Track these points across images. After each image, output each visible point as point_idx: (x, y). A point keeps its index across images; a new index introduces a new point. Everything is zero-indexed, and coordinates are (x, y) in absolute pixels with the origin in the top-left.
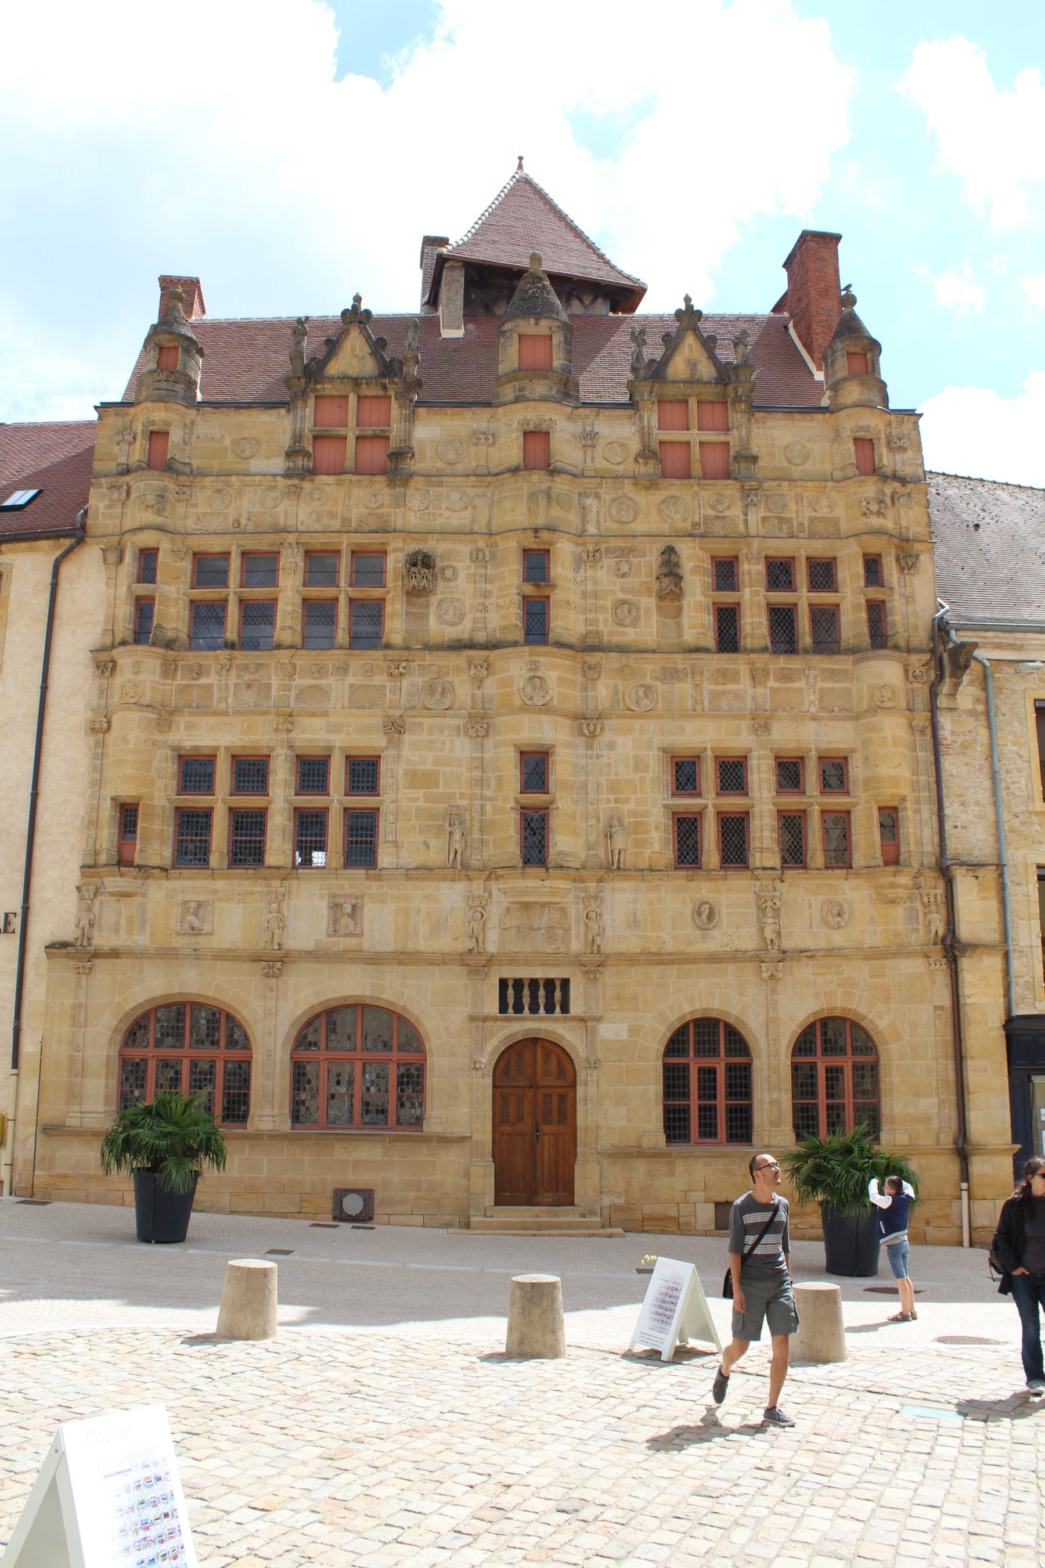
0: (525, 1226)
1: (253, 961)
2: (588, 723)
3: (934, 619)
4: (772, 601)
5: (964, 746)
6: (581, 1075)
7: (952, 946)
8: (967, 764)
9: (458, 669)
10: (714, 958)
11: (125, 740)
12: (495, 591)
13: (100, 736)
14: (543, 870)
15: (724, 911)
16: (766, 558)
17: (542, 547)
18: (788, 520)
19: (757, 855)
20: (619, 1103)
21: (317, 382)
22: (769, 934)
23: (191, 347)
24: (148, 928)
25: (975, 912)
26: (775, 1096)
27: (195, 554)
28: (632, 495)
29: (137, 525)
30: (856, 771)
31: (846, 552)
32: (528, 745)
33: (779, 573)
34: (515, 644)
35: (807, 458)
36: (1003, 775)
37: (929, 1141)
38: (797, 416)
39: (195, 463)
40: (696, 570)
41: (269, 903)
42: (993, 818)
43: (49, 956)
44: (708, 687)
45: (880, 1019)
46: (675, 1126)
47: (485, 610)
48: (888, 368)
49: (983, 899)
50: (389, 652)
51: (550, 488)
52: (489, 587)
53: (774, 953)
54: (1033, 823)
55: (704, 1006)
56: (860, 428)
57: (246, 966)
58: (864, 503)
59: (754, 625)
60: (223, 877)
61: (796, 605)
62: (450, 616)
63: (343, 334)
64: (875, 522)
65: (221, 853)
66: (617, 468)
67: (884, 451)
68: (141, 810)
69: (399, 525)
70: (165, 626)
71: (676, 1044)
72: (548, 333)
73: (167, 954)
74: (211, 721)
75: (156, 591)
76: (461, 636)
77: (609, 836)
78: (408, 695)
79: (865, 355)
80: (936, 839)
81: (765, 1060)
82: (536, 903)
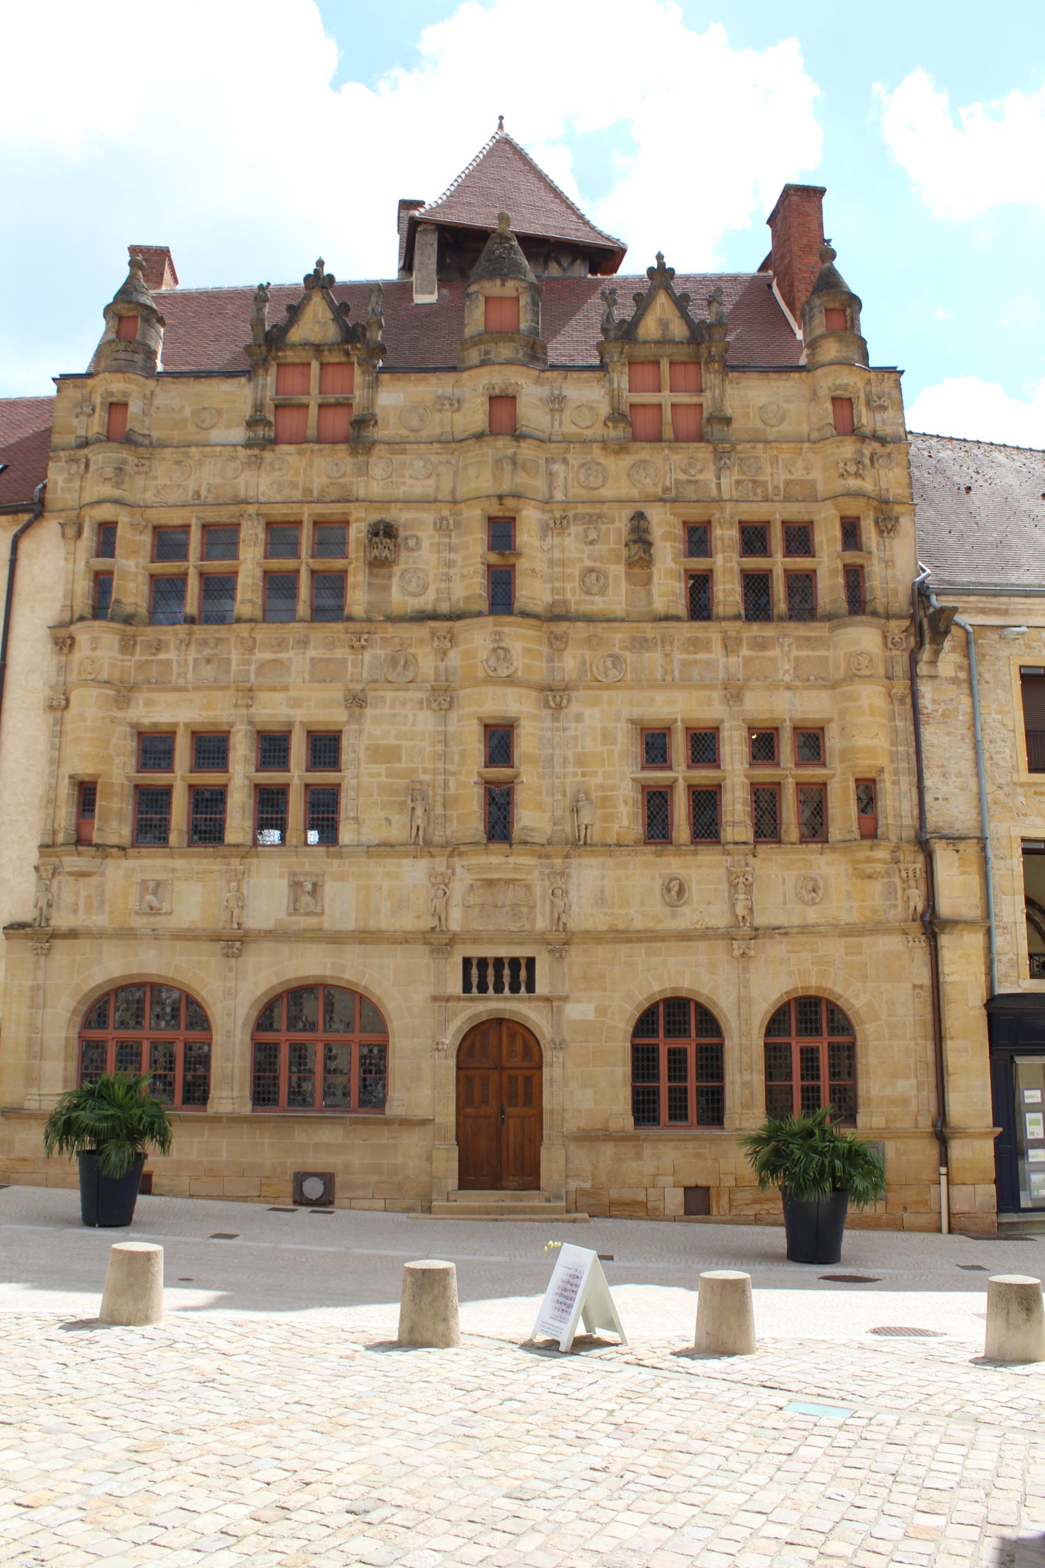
0: (487, 1211)
1: (212, 940)
2: (554, 694)
3: (914, 584)
4: (746, 567)
5: (945, 715)
6: (547, 1056)
7: (931, 923)
8: (948, 734)
9: (421, 641)
10: (684, 936)
11: (83, 718)
12: (459, 563)
13: (59, 714)
14: (507, 846)
15: (694, 887)
16: (740, 522)
17: (507, 514)
18: (764, 484)
19: (729, 829)
20: (586, 1084)
21: (278, 350)
22: (740, 911)
23: (151, 316)
24: (107, 908)
25: (955, 887)
26: (747, 1077)
27: (155, 528)
28: (601, 460)
29: (95, 499)
30: (833, 742)
31: (823, 515)
32: (491, 718)
33: (754, 538)
34: (479, 614)
35: (783, 418)
36: (986, 745)
37: (907, 1124)
38: (772, 375)
39: (155, 434)
40: (667, 536)
41: (229, 881)
42: (975, 790)
43: (8, 937)
44: (678, 656)
45: (856, 998)
46: (644, 1109)
47: (449, 579)
48: (868, 324)
49: (964, 873)
50: (350, 625)
51: (515, 454)
52: (453, 556)
53: (746, 930)
54: (1018, 794)
55: (674, 985)
56: (838, 387)
57: (205, 946)
58: (841, 465)
59: (727, 592)
61: (771, 571)
62: (413, 587)
63: (307, 299)
64: (853, 483)
65: (180, 832)
66: (586, 432)
67: (864, 410)
68: (99, 787)
69: (362, 493)
70: (124, 600)
71: (646, 1022)
72: (514, 294)
73: (126, 935)
74: (171, 697)
75: (114, 565)
76: (425, 608)
77: (575, 811)
78: (370, 668)
79: (844, 311)
80: (916, 812)
81: (736, 1041)
82: (499, 880)
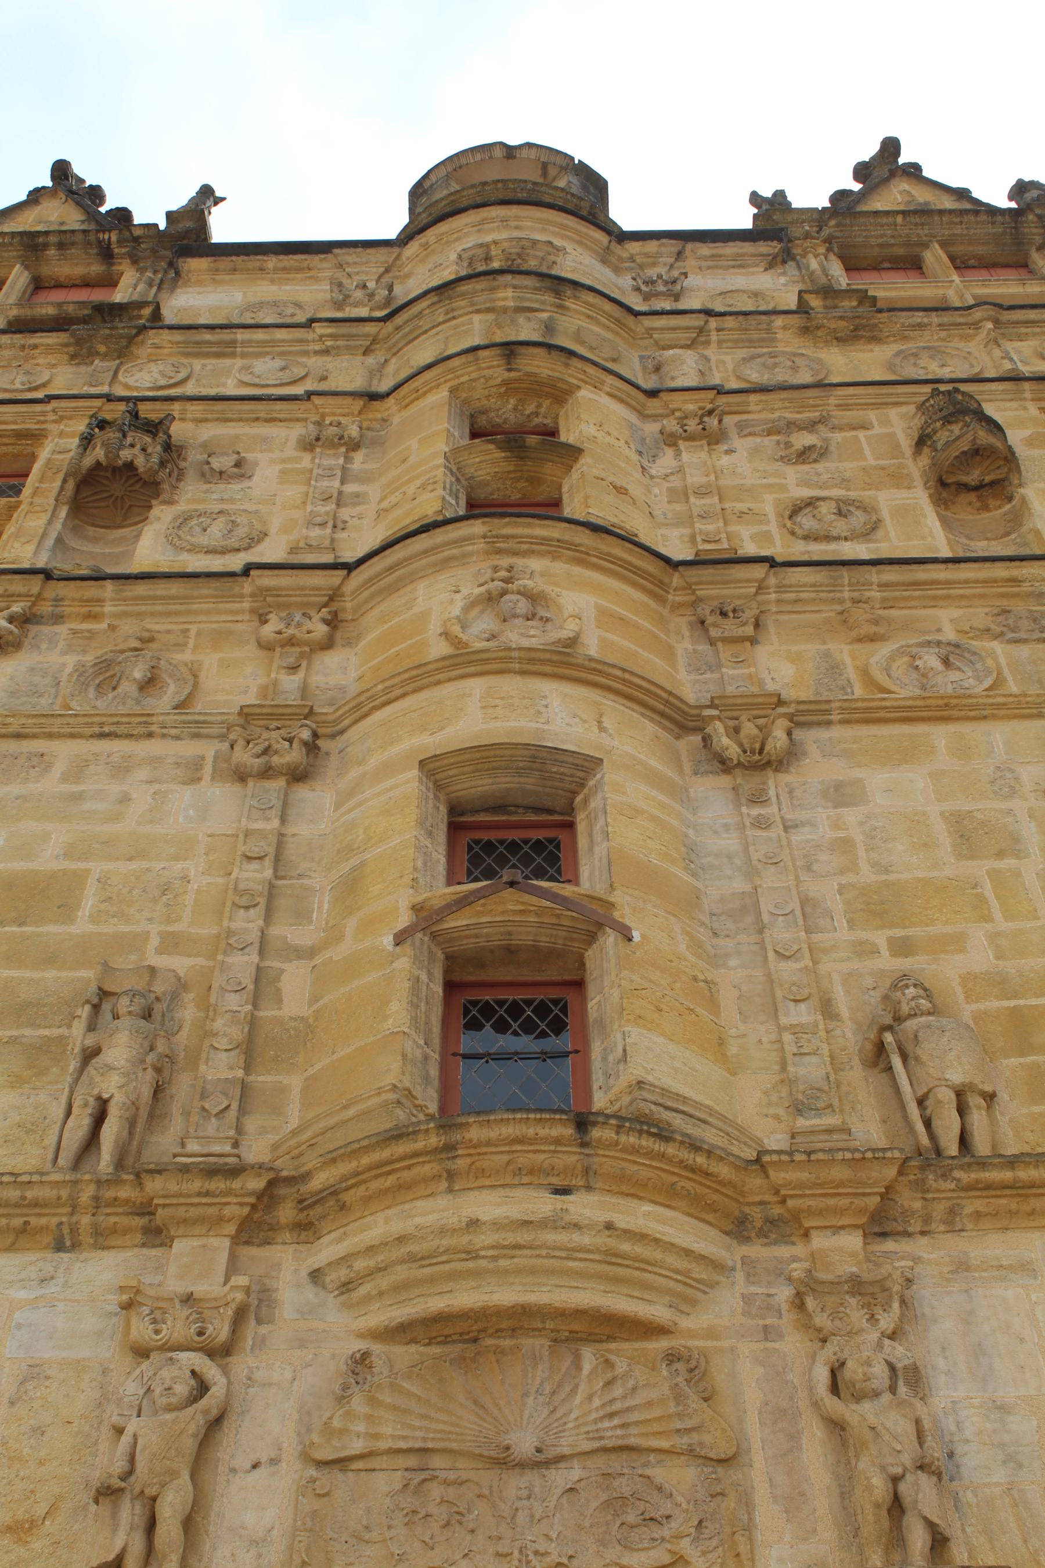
9: (219, 638)
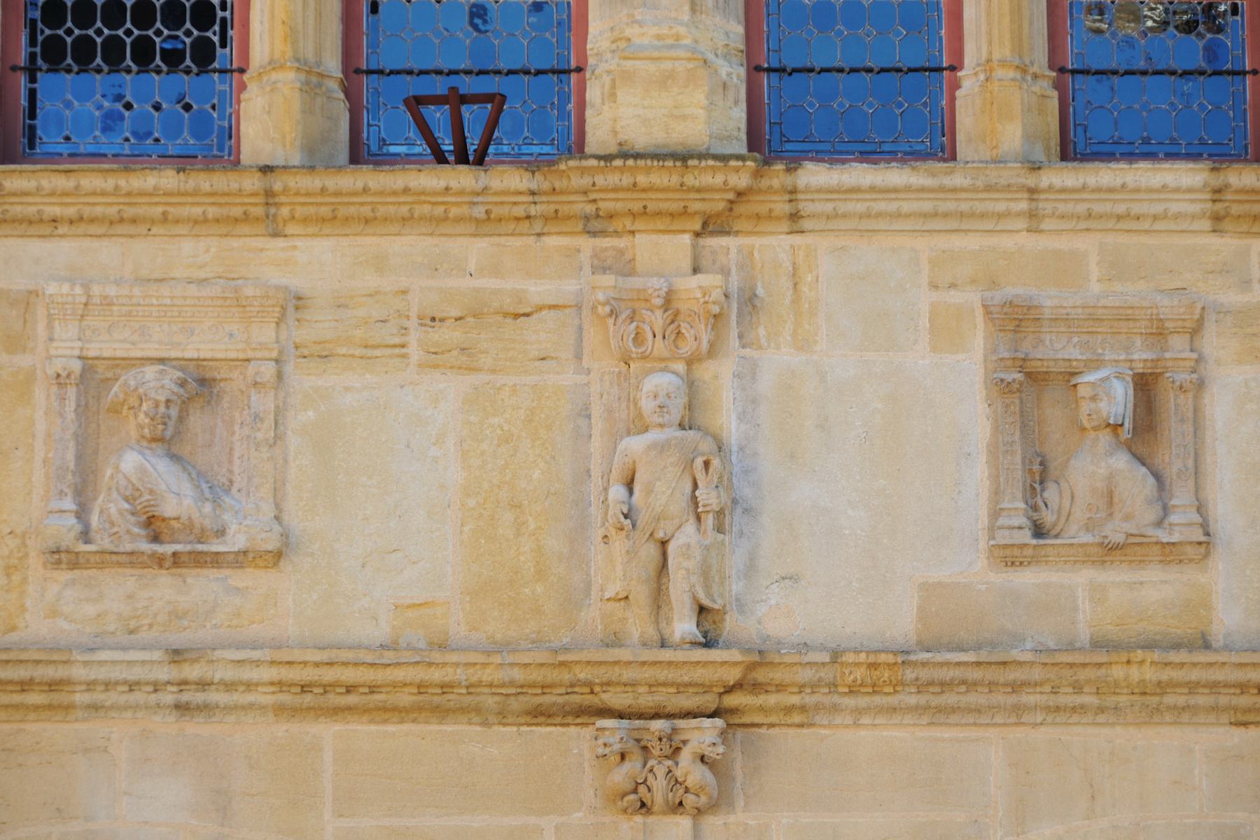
1: (540, 715)
57: (497, 748)
60: (332, 219)
